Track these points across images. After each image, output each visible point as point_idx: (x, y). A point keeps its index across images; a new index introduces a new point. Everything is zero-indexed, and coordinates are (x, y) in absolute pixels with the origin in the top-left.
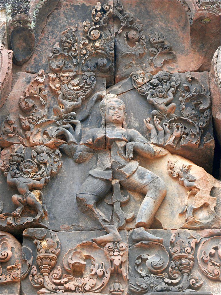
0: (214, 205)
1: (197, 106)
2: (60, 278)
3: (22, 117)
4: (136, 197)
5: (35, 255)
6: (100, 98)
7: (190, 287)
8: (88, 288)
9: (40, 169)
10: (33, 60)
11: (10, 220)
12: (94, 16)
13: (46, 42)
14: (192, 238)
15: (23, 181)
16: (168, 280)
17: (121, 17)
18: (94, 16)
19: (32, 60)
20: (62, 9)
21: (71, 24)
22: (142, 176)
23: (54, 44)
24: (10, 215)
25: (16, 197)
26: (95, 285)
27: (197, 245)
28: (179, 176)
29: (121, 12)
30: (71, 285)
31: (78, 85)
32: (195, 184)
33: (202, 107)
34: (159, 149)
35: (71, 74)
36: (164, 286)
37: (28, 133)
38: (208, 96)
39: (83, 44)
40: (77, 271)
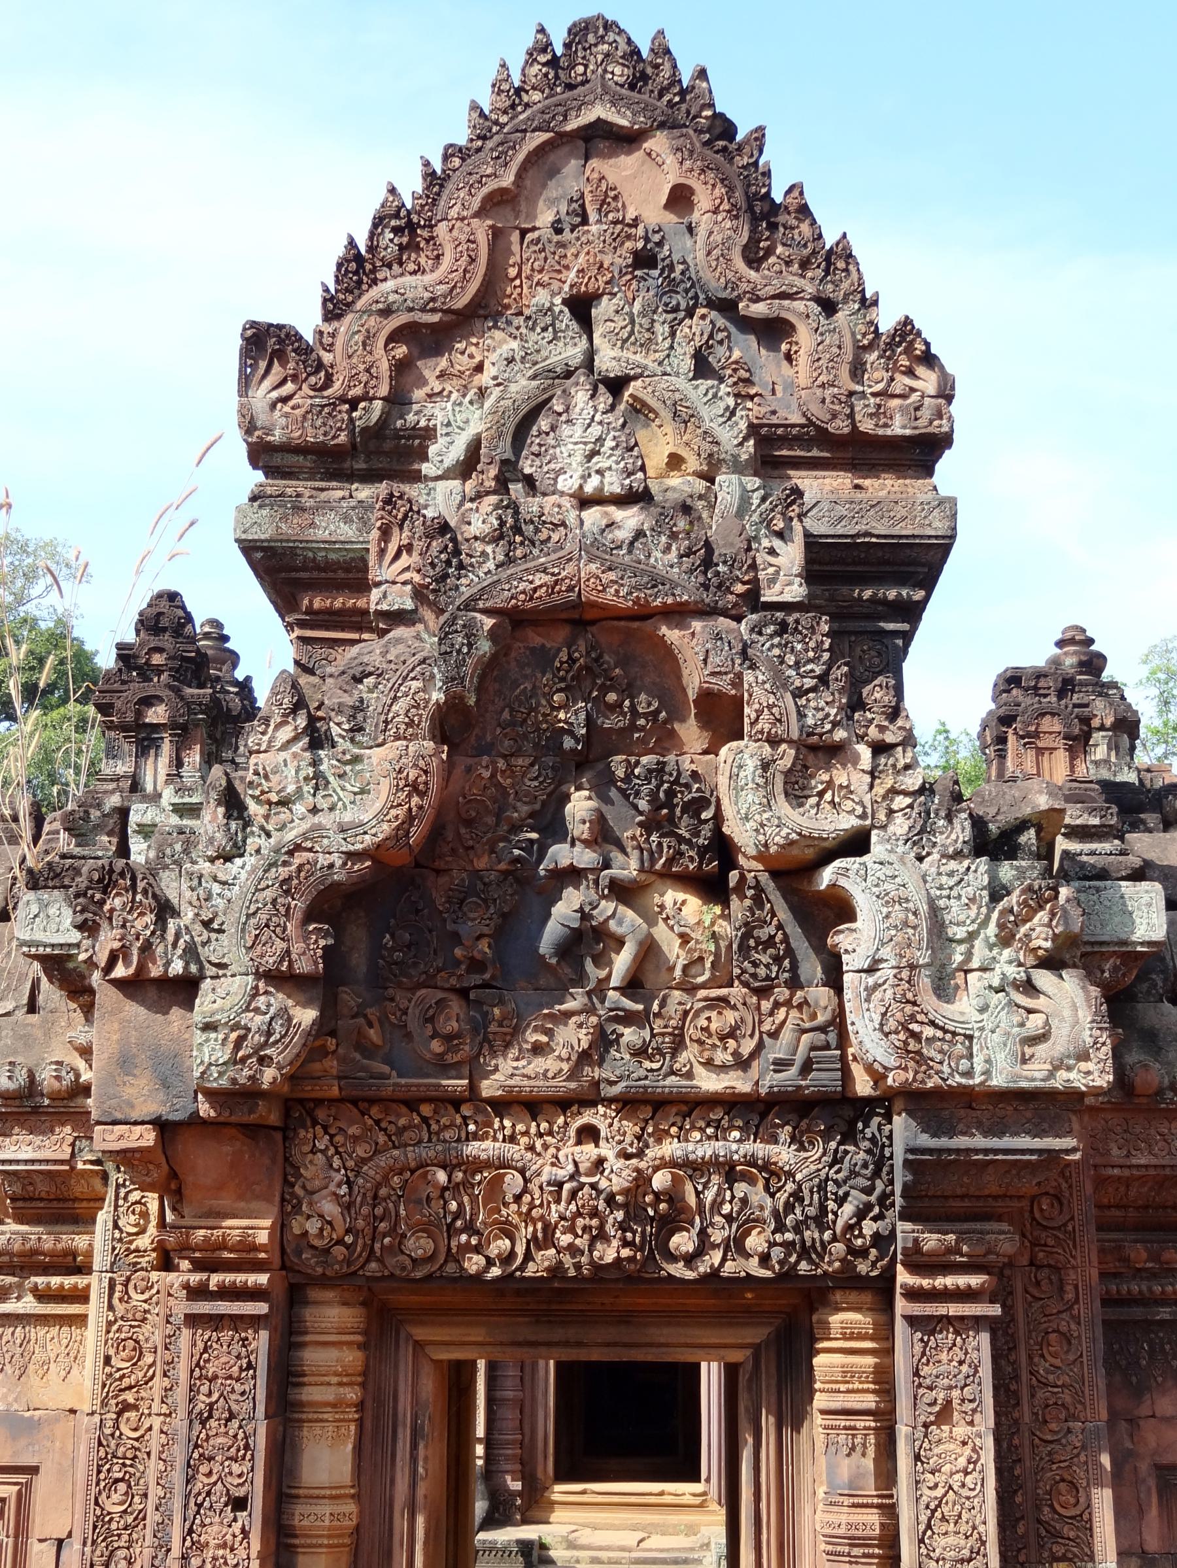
0: (711, 958)
1: (697, 815)
2: (517, 1059)
3: (463, 831)
4: (612, 944)
5: (486, 1027)
6: (567, 798)
7: (673, 1073)
8: (550, 1074)
9: (488, 908)
10: (473, 739)
11: (453, 981)
12: (559, 669)
13: (491, 708)
14: (680, 1003)
15: (467, 929)
16: (647, 1064)
17: (597, 670)
18: (559, 669)
19: (473, 739)
20: (513, 654)
21: (526, 677)
22: (620, 923)
23: (503, 710)
24: (453, 974)
25: (458, 952)
26: (561, 1070)
27: (686, 1013)
28: (668, 918)
29: (596, 660)
30: (529, 1070)
31: (536, 778)
32: (688, 930)
33: (703, 816)
34: (643, 877)
35: (528, 761)
36: (642, 1073)
37: (471, 853)
38: (713, 800)
39: (545, 715)
40: (538, 1050)
